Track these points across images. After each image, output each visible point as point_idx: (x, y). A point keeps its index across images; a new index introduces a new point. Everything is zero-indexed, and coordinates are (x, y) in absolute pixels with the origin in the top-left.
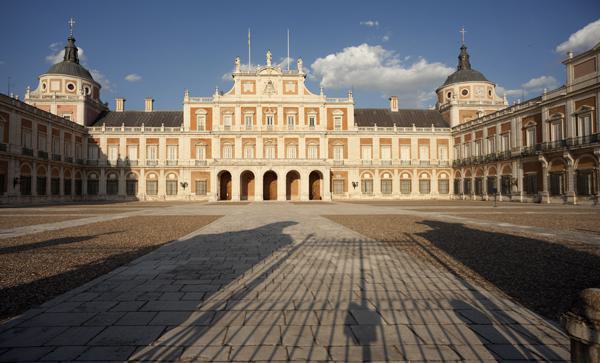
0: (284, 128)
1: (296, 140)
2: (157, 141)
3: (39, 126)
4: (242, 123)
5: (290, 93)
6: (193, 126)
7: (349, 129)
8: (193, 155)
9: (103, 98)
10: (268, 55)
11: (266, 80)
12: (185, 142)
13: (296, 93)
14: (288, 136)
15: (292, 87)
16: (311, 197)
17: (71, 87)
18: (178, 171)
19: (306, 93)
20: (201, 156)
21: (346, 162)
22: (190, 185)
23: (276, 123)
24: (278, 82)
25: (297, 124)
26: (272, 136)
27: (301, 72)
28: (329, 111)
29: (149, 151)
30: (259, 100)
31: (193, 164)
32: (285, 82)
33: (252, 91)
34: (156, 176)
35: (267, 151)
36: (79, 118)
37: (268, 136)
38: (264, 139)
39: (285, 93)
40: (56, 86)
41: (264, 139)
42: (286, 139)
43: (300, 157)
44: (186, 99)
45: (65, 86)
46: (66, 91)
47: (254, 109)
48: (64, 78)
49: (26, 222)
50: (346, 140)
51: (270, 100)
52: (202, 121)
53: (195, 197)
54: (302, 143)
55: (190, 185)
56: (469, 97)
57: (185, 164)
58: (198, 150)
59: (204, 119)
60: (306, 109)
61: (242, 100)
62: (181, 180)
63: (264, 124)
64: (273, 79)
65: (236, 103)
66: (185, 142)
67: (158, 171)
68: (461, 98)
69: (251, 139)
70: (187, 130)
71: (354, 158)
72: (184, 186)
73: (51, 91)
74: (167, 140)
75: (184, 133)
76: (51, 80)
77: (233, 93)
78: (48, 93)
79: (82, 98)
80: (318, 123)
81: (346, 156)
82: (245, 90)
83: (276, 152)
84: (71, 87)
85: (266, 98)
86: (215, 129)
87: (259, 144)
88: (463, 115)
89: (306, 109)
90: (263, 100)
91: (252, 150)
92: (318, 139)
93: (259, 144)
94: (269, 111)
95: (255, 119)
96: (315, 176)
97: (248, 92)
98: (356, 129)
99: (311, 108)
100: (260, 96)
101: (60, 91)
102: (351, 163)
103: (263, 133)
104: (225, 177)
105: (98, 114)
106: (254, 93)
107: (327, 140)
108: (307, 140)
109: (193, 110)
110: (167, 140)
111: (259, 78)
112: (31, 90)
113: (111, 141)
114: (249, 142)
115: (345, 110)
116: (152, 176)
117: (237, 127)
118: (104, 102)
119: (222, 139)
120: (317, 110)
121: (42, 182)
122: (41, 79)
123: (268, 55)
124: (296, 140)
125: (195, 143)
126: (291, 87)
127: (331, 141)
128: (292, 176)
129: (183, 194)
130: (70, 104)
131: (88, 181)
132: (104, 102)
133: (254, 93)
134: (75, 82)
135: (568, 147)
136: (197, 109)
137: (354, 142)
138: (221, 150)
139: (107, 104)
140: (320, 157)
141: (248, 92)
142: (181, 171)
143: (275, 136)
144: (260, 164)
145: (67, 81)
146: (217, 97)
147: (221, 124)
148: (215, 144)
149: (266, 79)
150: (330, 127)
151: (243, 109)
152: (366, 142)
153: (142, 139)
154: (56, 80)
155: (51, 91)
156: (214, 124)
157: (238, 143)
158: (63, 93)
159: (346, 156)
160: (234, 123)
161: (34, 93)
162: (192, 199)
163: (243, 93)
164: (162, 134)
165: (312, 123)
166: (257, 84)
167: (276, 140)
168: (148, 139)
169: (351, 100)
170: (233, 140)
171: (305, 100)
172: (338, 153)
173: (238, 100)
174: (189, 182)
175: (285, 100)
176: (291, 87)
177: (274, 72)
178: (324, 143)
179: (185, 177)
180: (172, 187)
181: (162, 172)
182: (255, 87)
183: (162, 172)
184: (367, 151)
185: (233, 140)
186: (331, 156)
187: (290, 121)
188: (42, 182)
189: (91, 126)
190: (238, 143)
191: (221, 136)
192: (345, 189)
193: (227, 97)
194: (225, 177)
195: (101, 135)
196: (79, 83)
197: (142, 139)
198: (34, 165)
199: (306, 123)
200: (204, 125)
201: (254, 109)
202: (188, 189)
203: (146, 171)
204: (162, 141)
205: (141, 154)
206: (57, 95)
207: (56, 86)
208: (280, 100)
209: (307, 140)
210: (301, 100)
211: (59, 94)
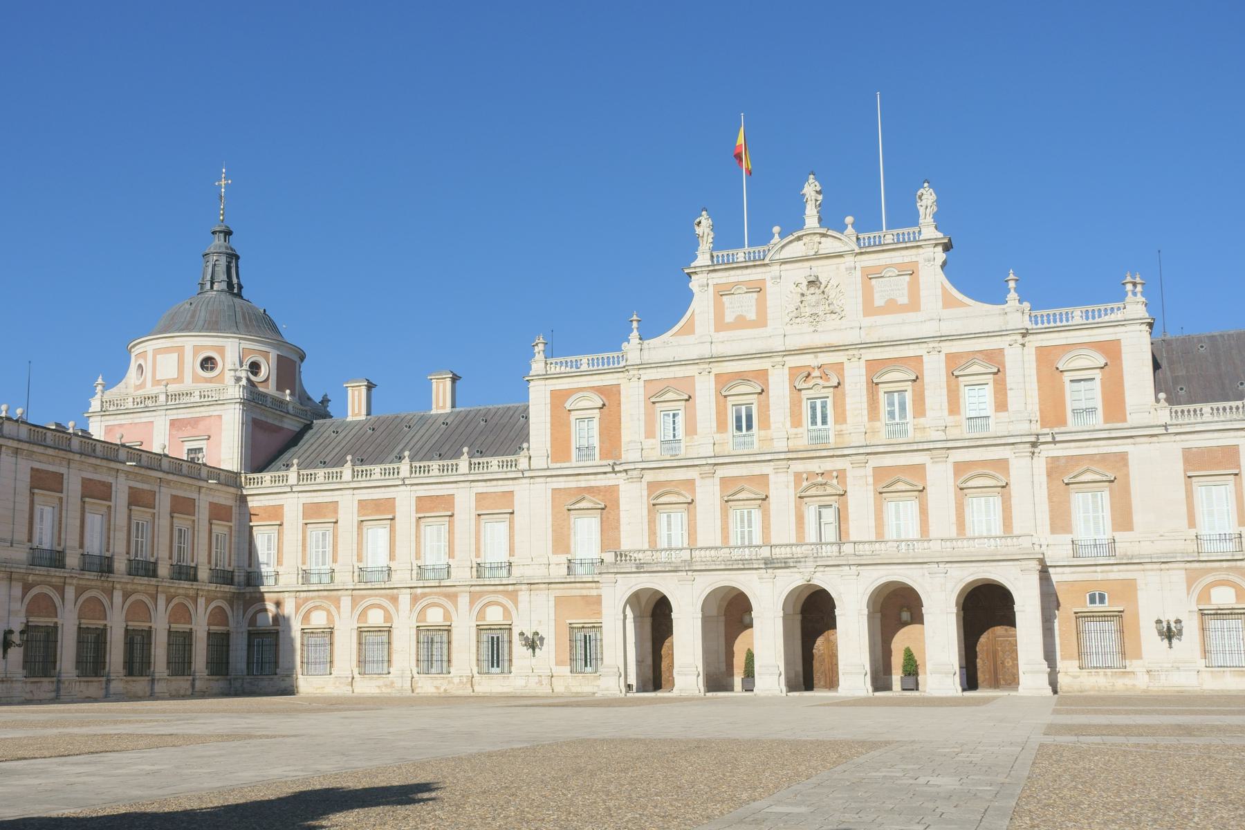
0: (875, 432)
1: (919, 469)
2: (448, 501)
3: (86, 483)
4: (721, 426)
5: (891, 307)
6: (560, 448)
7: (1132, 420)
8: (561, 541)
9: (314, 383)
10: (811, 189)
11: (800, 273)
12: (533, 500)
13: (914, 304)
14: (888, 461)
15: (898, 289)
16: (970, 682)
18: (513, 596)
19: (948, 303)
21: (1127, 543)
22: (550, 641)
23: (841, 418)
24: (843, 277)
25: (920, 411)
26: (828, 465)
27: (929, 231)
28: (1046, 357)
30: (778, 345)
31: (560, 572)
32: (870, 275)
33: (752, 316)
34: (447, 615)
36: (226, 451)
37: (814, 466)
38: (798, 475)
39: (869, 309)
40: (167, 367)
41: (798, 475)
42: (879, 472)
43: (934, 532)
44: (537, 366)
45: (192, 363)
46: (196, 379)
47: (763, 375)
49: (101, 748)
50: (1122, 458)
52: (586, 432)
53: (568, 683)
54: (940, 478)
55: (550, 641)
57: (536, 573)
59: (595, 424)
60: (951, 358)
61: (719, 350)
62: (523, 625)
63: (796, 423)
64: (823, 270)
66: (533, 500)
67: (453, 597)
69: (750, 478)
72: (533, 644)
73: (156, 382)
74: (480, 497)
75: (529, 475)
76: (157, 352)
77: (689, 329)
78: (150, 390)
79: (236, 392)
81: (1123, 519)
82: (729, 318)
83: (841, 517)
84: (208, 363)
85: (803, 336)
86: (629, 454)
89: (951, 358)
90: (793, 343)
91: (757, 515)
92: (1002, 465)
94: (816, 380)
96: (985, 608)
97: (741, 323)
98: (1163, 414)
99: (973, 356)
100: (782, 331)
101: (180, 379)
102: (1147, 548)
103: (793, 455)
104: (656, 617)
105: (282, 429)
106: (761, 322)
107: (1040, 464)
109: (558, 399)
110: (480, 497)
111: (775, 269)
112: (106, 387)
113: (314, 513)
114: (745, 491)
115: (1111, 350)
116: (435, 617)
118: (317, 399)
119: (651, 485)
120: (994, 359)
121: (137, 644)
122: (135, 351)
123: (811, 189)
124: (919, 469)
125: (567, 505)
126: (892, 288)
127: (1055, 469)
128: (896, 608)
129: (529, 672)
130: (203, 412)
131: (250, 634)
132: (317, 399)
133: (761, 322)
134: (221, 350)
136: (569, 393)
137: (1155, 466)
138: (652, 523)
139: (325, 401)
140: (998, 532)
141: (741, 323)
142: (523, 596)
143: (839, 464)
145: (197, 349)
146: (632, 348)
147: (650, 433)
148: (632, 499)
149: (800, 273)
153: (405, 500)
154: (167, 350)
155: (156, 382)
156: (626, 435)
157: (708, 494)
158: (188, 384)
159: (1123, 519)
160: (691, 430)
161: (109, 395)
162: (559, 688)
163: (720, 325)
164: (463, 482)
166: (770, 288)
167: (841, 475)
168: (419, 499)
169: (1136, 307)
170: (690, 483)
171: (946, 329)
173: (705, 351)
174: (548, 632)
176: (892, 288)
177: (829, 245)
179: (535, 614)
180: (495, 651)
181: (464, 600)
182: (762, 308)
183: (464, 600)
185: (690, 483)
186: (1060, 520)
188: (137, 644)
189: (261, 469)
190: (708, 494)
191: (649, 476)
192: (1126, 648)
193: (666, 346)
194: (656, 617)
195: (280, 497)
196: (231, 350)
197: (405, 500)
198: (118, 596)
200: (596, 442)
201: (763, 375)
202: (547, 652)
203: (415, 599)
204: (464, 499)
205: (398, 551)
206: (173, 394)
207: (167, 367)
208: (852, 337)
209: (959, 468)
210: (928, 329)
211: (172, 388)
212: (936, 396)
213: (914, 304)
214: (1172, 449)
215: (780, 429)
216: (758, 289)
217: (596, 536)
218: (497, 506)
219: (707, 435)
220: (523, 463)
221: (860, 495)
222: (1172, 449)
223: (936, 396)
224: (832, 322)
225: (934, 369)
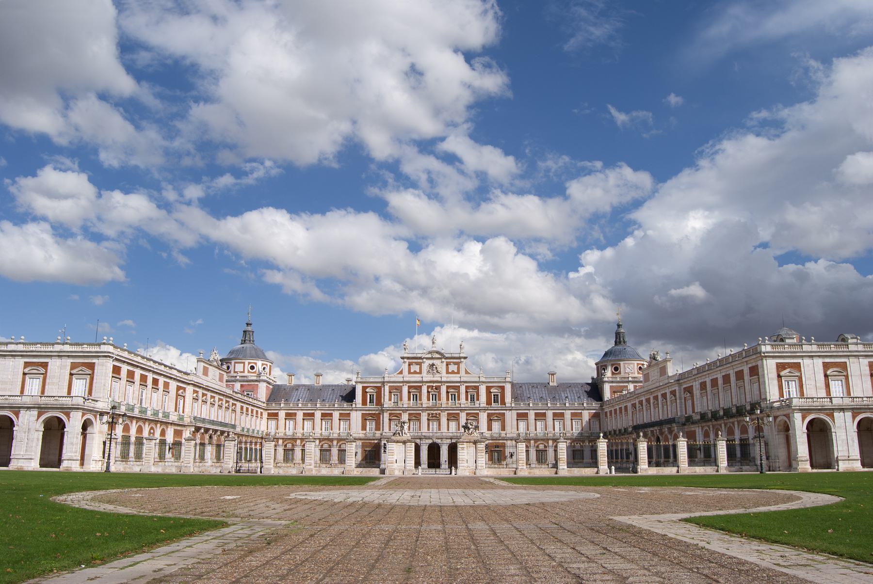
2: (331, 415)
5: (453, 372)
6: (364, 402)
8: (364, 428)
17: (252, 368)
20: (371, 429)
23: (440, 400)
25: (459, 399)
29: (324, 423)
30: (425, 379)
35: (431, 426)
38: (429, 415)
39: (448, 372)
42: (449, 414)
45: (247, 367)
46: (249, 372)
47: (421, 387)
48: (247, 362)
51: (435, 379)
56: (620, 373)
58: (368, 423)
60: (467, 387)
63: (429, 399)
65: (403, 382)
66: (356, 417)
68: (613, 373)
70: (359, 405)
71: (511, 430)
73: (235, 372)
80: (478, 399)
81: (503, 428)
84: (252, 368)
87: (424, 417)
88: (614, 392)
93: (424, 417)
94: (435, 390)
95: (420, 395)
97: (415, 372)
101: (244, 372)
106: (420, 373)
108: (467, 414)
109: (364, 388)
115: (503, 388)
117: (405, 402)
120: (477, 388)
125: (364, 418)
127: (489, 415)
135: (694, 423)
136: (367, 387)
137: (511, 417)
141: (415, 372)
144: (426, 438)
147: (390, 400)
149: (431, 362)
150: (489, 402)
151: (410, 387)
152: (522, 416)
155: (235, 372)
158: (246, 374)
159: (503, 428)
165: (472, 399)
170: (400, 414)
172: (496, 426)
173: (406, 379)
175: (448, 380)
178: (483, 417)
184: (522, 425)
187: (456, 397)
199: (467, 399)
208: (444, 379)
212: (463, 396)
213: (458, 372)
214: (514, 413)
215: (425, 402)
216: (420, 364)
217: (374, 426)
218: (345, 417)
219: (405, 402)
220: (354, 406)
221: (444, 420)
222: (514, 413)
223: (463, 396)
224: (438, 375)
225: (463, 389)
